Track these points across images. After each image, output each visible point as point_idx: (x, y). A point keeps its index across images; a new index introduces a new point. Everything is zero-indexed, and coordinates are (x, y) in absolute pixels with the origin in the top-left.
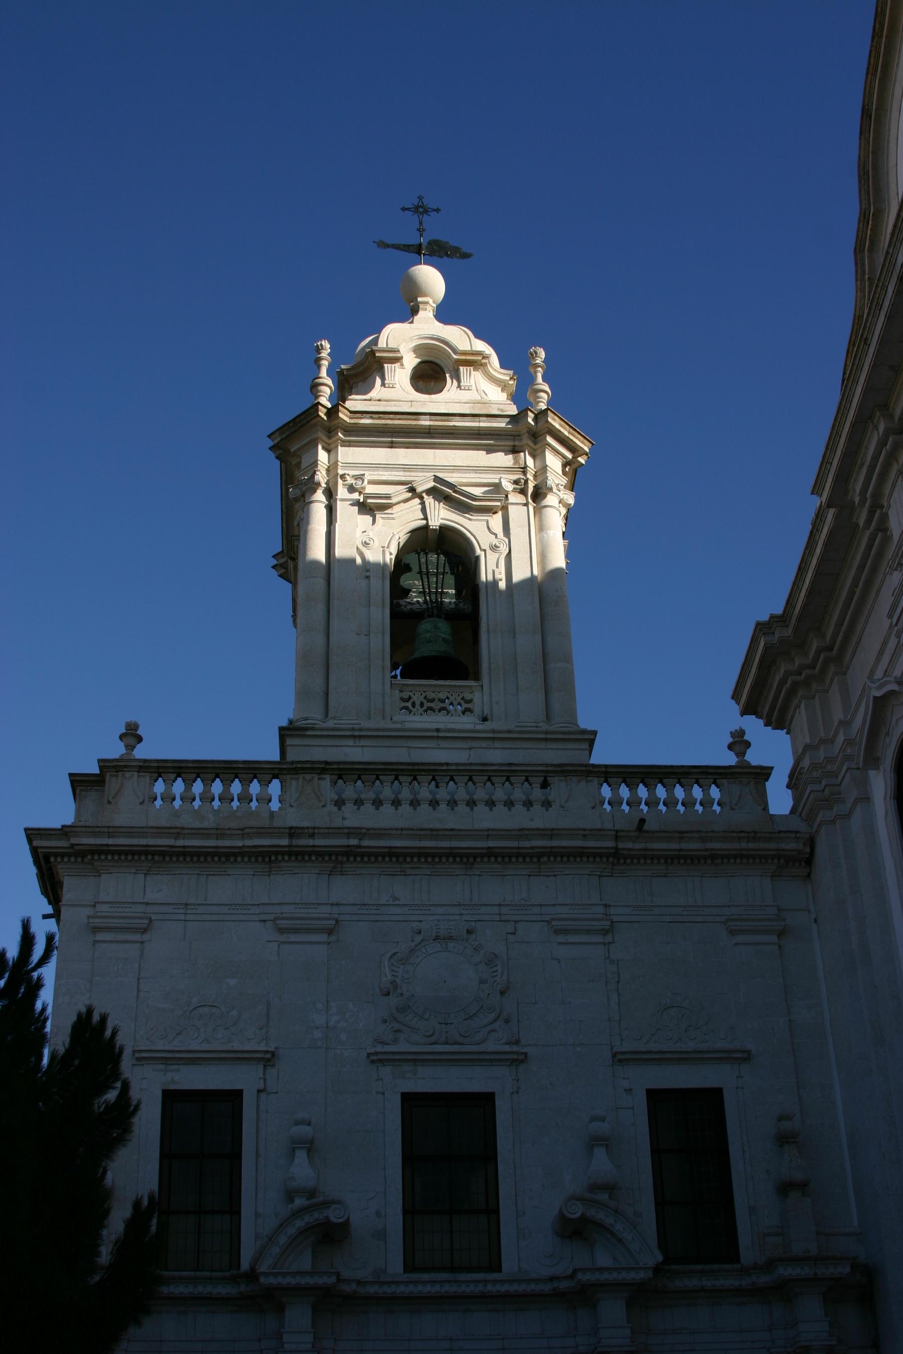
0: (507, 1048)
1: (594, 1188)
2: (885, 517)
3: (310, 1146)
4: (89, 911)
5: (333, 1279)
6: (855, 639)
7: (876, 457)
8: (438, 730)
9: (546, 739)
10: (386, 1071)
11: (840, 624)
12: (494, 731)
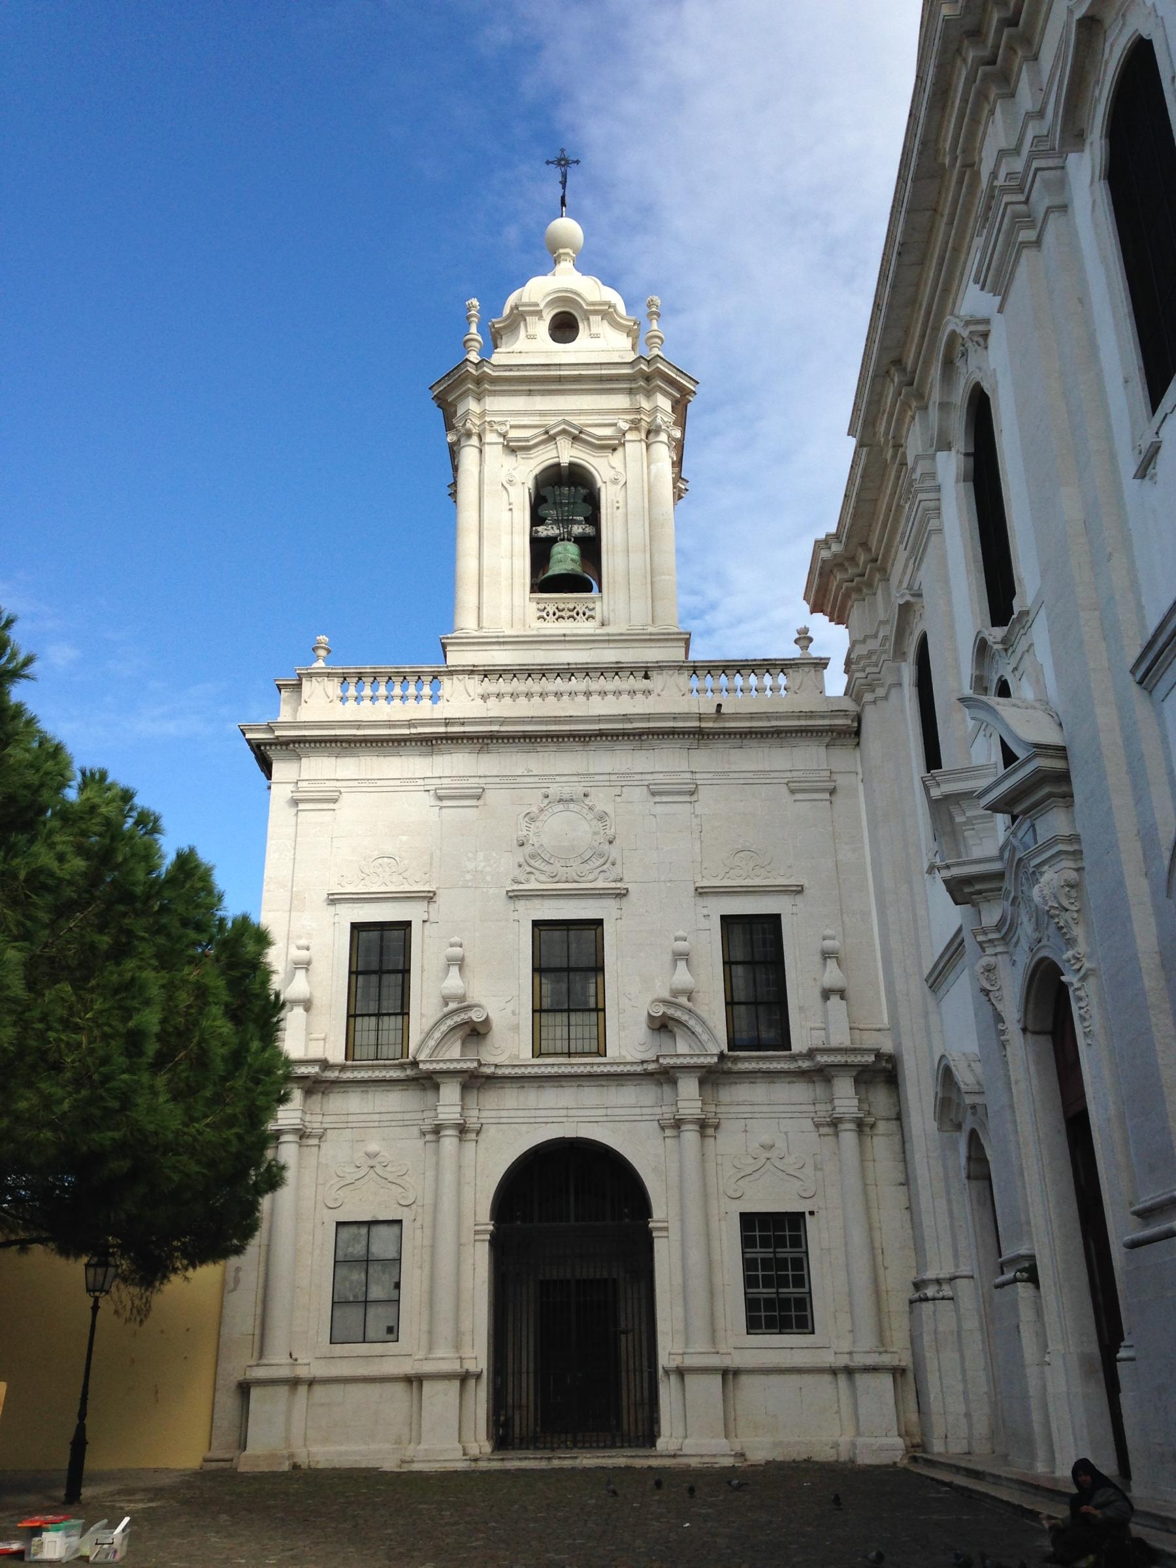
0: (613, 885)
1: (676, 993)
2: (904, 455)
3: (460, 963)
4: (291, 787)
5: (475, 1064)
6: (893, 551)
7: (894, 405)
8: (564, 635)
9: (650, 640)
10: (521, 904)
11: (880, 540)
12: (609, 635)
